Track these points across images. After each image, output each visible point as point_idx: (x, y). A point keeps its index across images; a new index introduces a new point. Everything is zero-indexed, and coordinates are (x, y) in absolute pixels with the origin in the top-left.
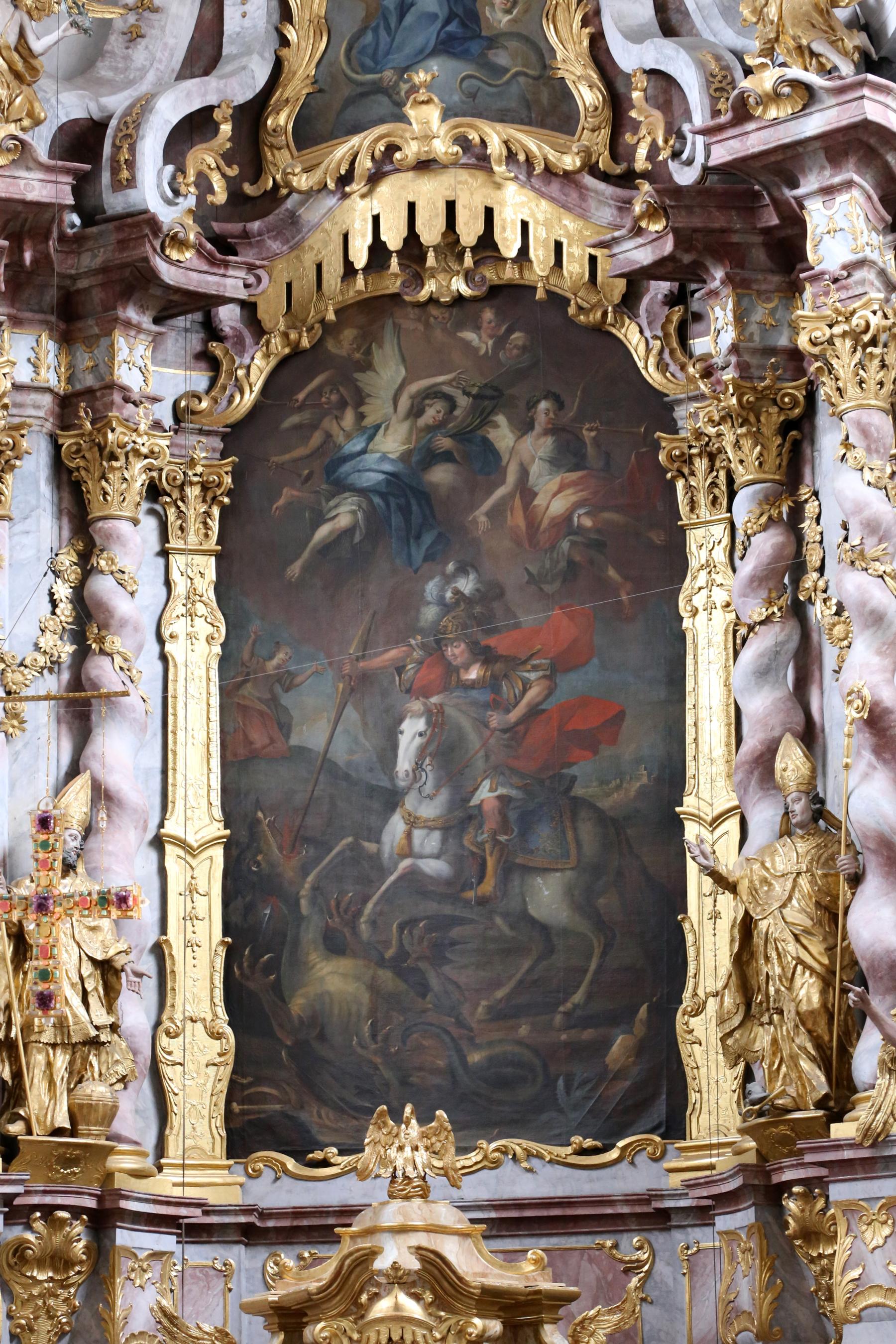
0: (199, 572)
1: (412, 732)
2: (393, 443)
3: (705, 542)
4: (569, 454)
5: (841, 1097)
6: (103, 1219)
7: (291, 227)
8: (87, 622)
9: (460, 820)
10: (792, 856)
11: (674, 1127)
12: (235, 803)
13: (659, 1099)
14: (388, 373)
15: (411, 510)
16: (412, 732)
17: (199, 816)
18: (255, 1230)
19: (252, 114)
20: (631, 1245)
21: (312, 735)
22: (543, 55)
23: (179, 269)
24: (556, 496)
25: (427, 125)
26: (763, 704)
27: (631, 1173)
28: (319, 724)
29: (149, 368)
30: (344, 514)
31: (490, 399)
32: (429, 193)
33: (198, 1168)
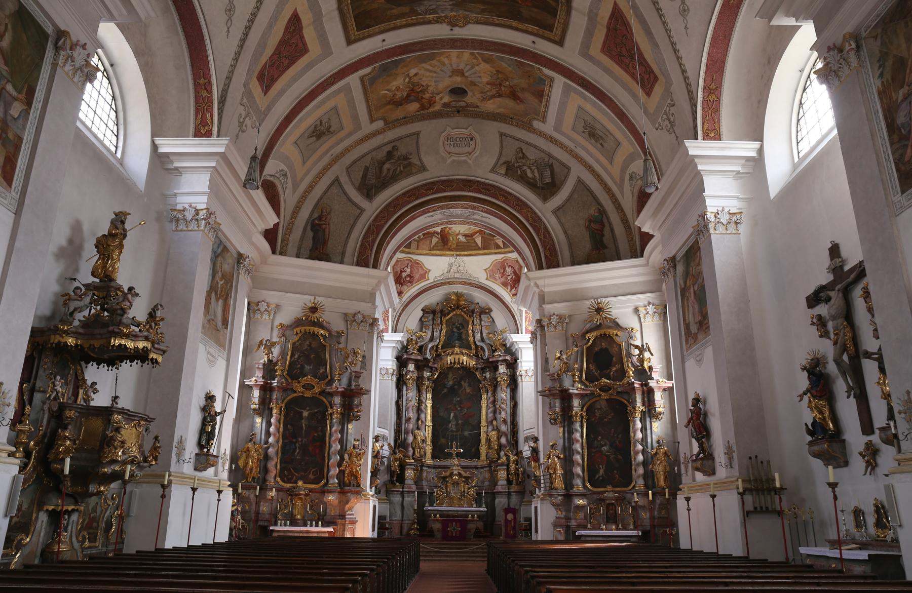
0: (429, 396)
1: (452, 415)
2: (451, 383)
3: (484, 396)
4: (470, 386)
5: (499, 458)
6: (422, 466)
7: (441, 359)
8: (420, 402)
9: (457, 425)
10: (494, 433)
11: (479, 458)
12: (433, 421)
13: (477, 455)
14: (451, 375)
15: (452, 391)
16: (452, 415)
17: (429, 422)
18: (435, 467)
19: (437, 346)
20: (474, 471)
21: (441, 414)
22: (468, 341)
23: (431, 364)
24: (468, 390)
25: (457, 350)
26: (491, 415)
27: (474, 463)
28: (442, 414)
29: (426, 374)
30: (445, 390)
31: (461, 379)
32: (457, 357)
33: (430, 462)
